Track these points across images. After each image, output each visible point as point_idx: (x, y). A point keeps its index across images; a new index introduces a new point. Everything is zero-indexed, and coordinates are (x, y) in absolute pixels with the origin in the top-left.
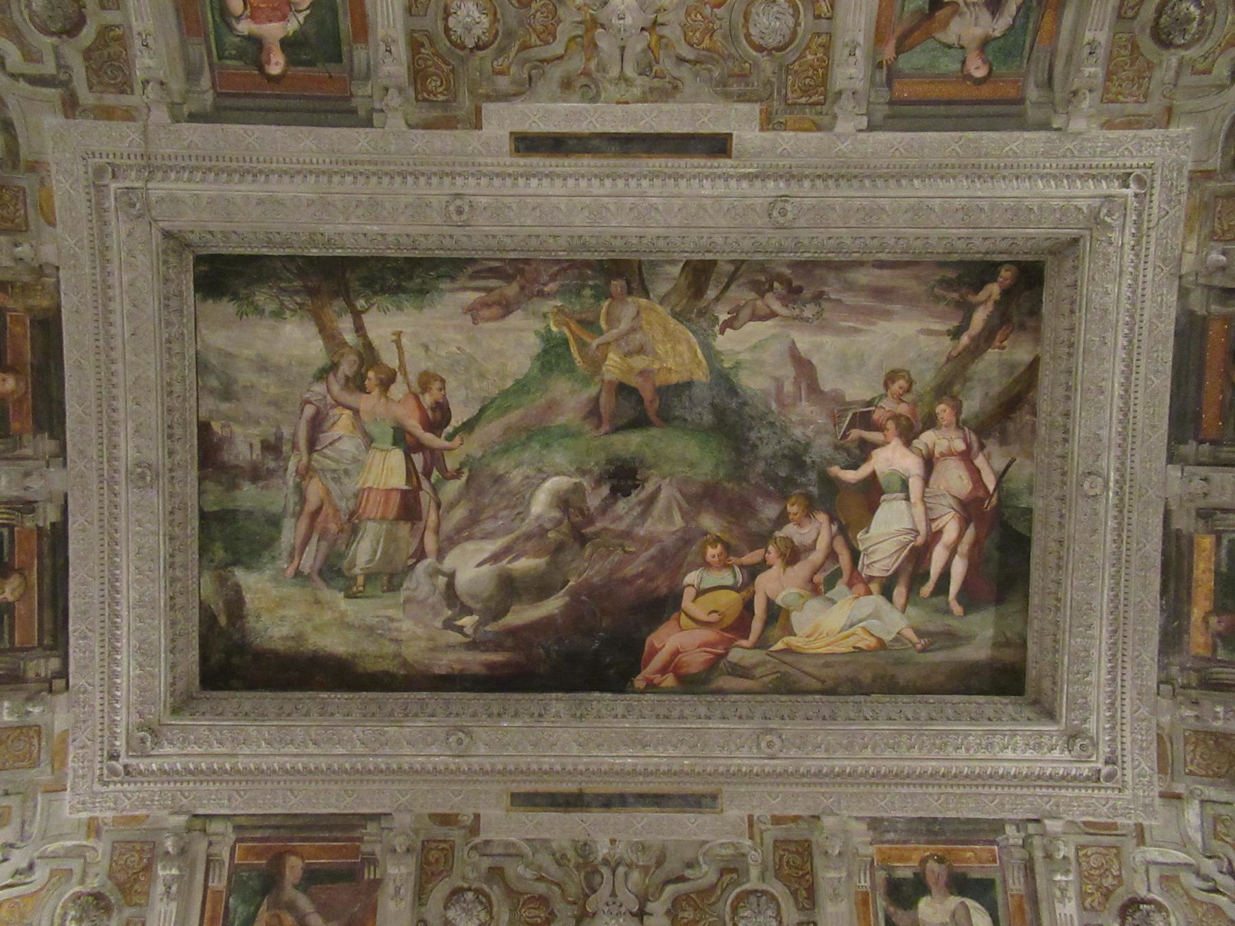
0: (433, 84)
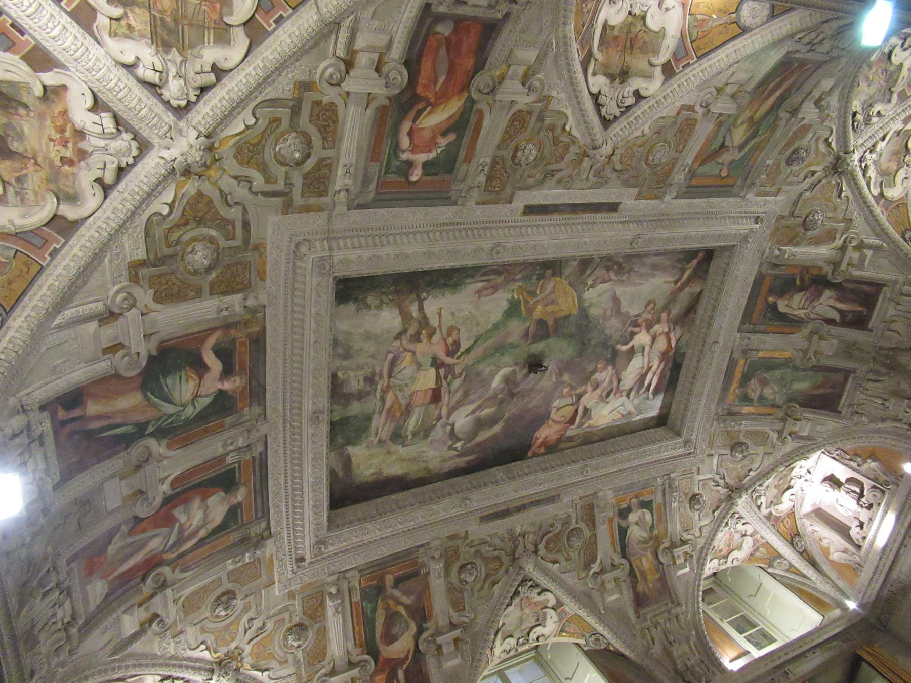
0: (495, 183)
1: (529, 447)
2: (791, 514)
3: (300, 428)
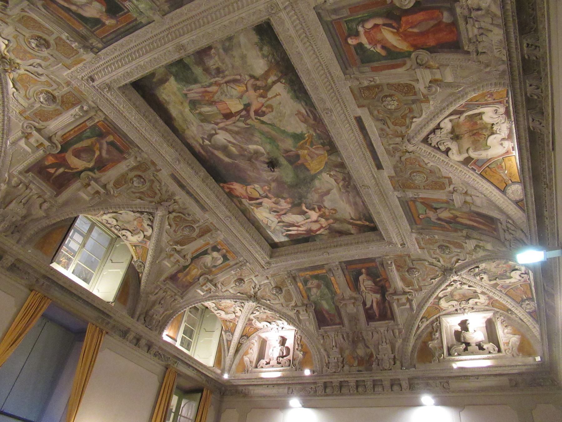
0: (367, 92)
1: (225, 182)
2: (257, 330)
3: (169, 41)
